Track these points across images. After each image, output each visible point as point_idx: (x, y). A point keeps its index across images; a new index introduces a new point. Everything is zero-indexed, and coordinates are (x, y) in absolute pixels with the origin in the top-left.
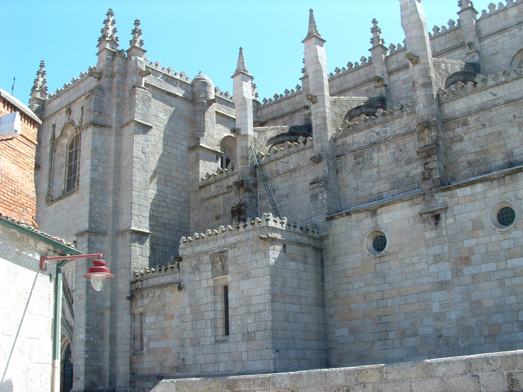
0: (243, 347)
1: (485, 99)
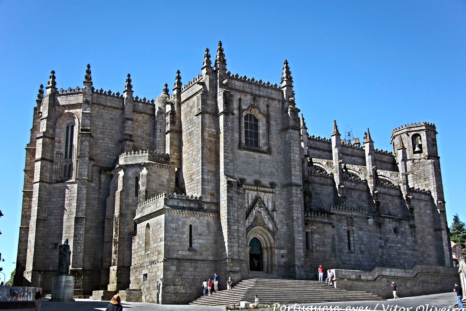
0: (360, 256)
1: (384, 191)
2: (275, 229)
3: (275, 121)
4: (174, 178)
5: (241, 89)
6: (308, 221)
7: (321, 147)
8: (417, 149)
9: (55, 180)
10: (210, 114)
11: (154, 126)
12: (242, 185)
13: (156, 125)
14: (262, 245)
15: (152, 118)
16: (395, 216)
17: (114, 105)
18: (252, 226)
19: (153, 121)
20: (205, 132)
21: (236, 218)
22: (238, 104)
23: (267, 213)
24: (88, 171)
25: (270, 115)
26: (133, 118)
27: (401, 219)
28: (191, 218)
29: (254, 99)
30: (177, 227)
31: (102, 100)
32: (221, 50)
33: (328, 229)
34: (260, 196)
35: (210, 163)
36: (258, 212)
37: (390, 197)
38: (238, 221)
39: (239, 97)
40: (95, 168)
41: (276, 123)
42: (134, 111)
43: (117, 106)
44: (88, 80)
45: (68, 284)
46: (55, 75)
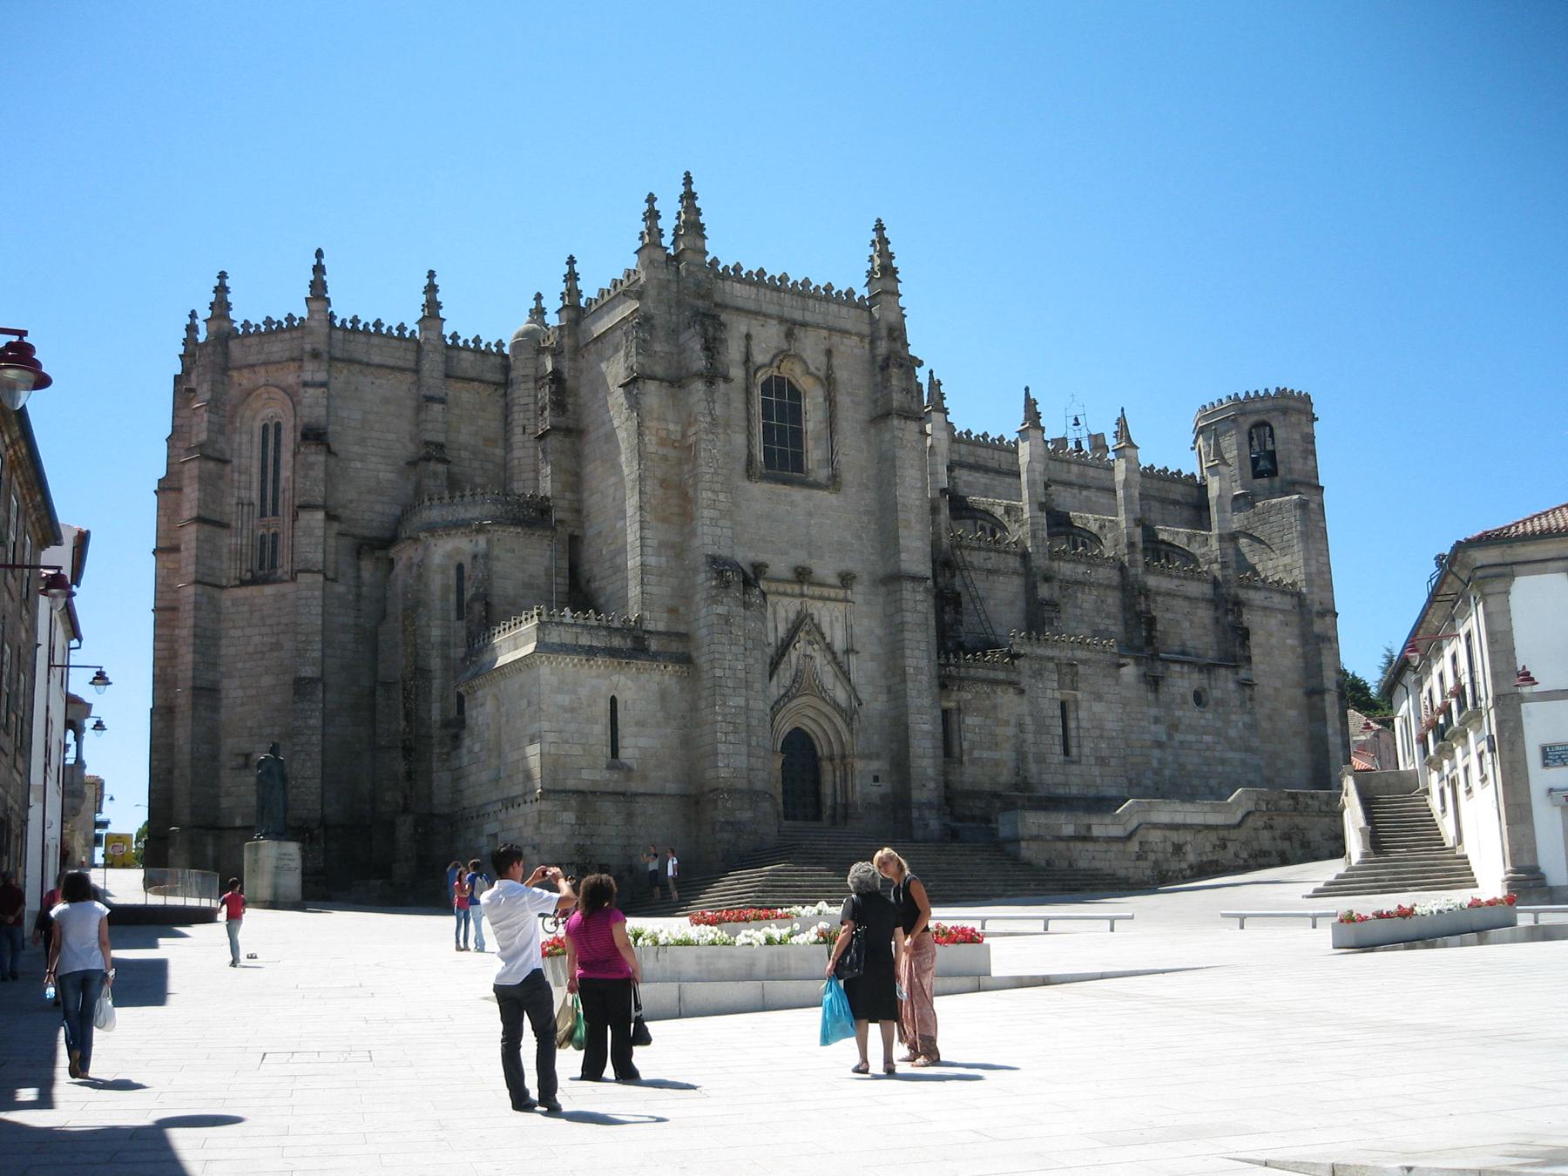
0: (1096, 771)
2: (855, 703)
3: (850, 394)
4: (565, 564)
5: (752, 306)
6: (950, 677)
7: (993, 464)
8: (1263, 464)
9: (235, 578)
10: (661, 380)
11: (506, 417)
12: (756, 579)
13: (511, 413)
14: (819, 750)
15: (501, 391)
16: (1197, 656)
17: (391, 362)
18: (788, 696)
19: (502, 402)
20: (647, 432)
21: (742, 675)
22: (743, 349)
23: (829, 657)
24: (324, 551)
25: (835, 379)
26: (447, 394)
27: (1214, 665)
28: (615, 678)
29: (789, 335)
30: (575, 705)
31: (358, 349)
32: (689, 197)
33: (1007, 701)
34: (810, 611)
35: (665, 520)
36: (805, 656)
37: (1186, 603)
38: (748, 685)
39: (744, 329)
40: (345, 541)
41: (852, 401)
42: (447, 376)
43: (400, 363)
44: (318, 290)
45: (286, 862)
46: (228, 283)
